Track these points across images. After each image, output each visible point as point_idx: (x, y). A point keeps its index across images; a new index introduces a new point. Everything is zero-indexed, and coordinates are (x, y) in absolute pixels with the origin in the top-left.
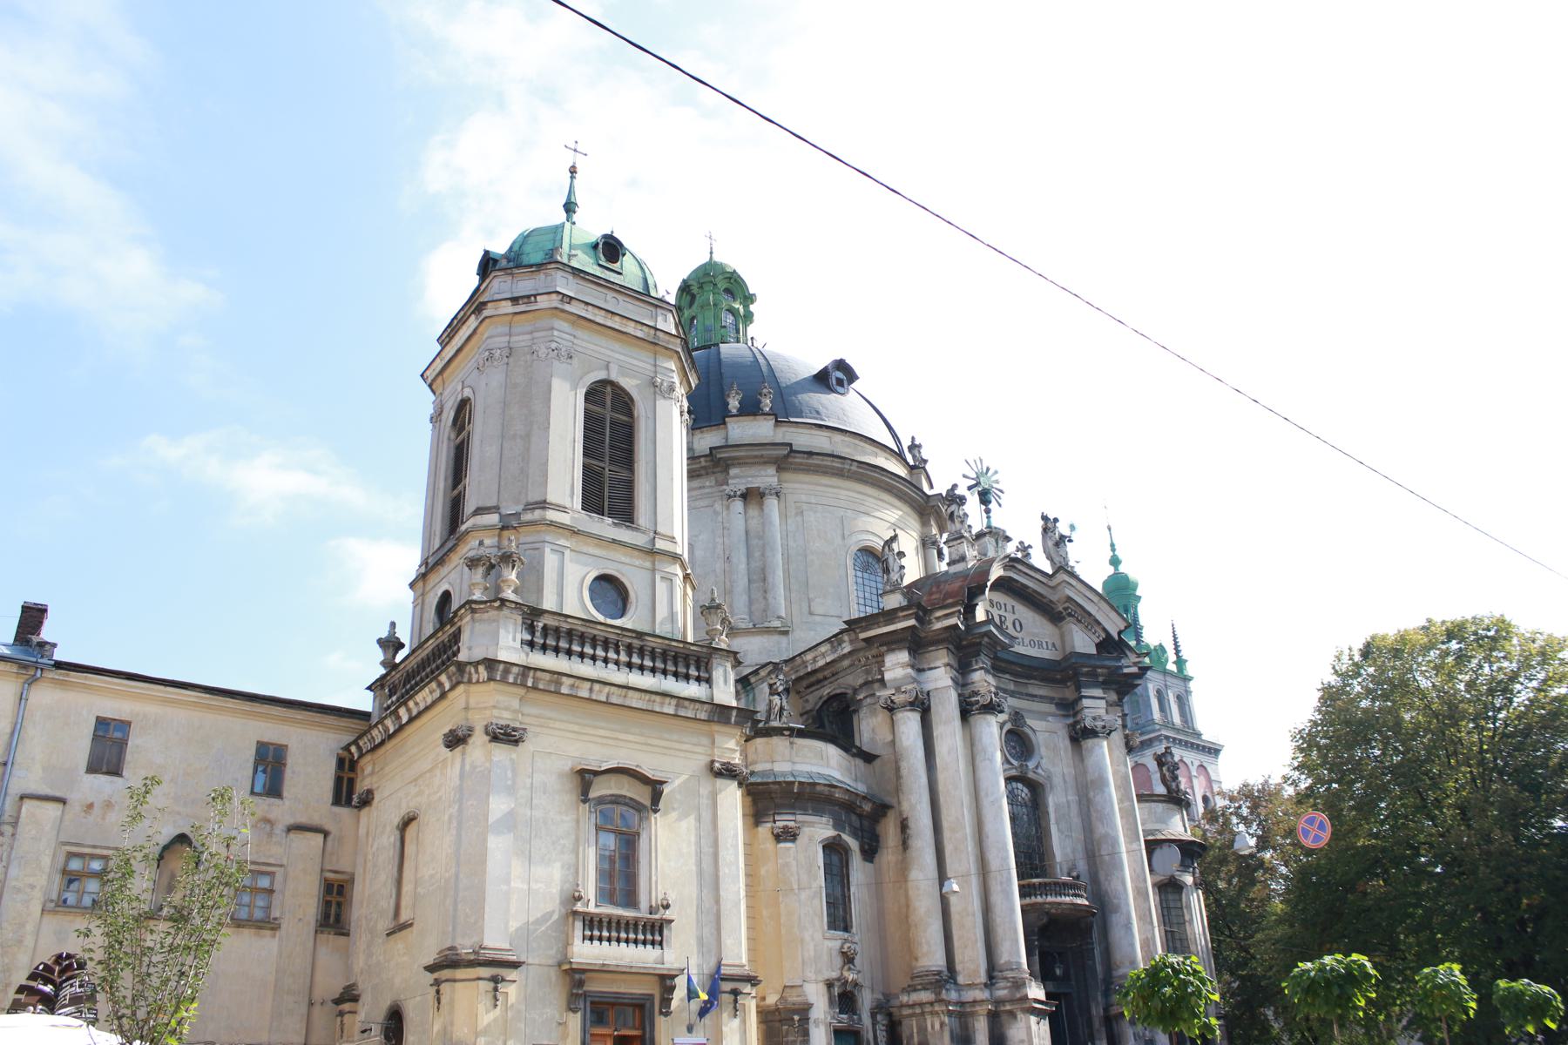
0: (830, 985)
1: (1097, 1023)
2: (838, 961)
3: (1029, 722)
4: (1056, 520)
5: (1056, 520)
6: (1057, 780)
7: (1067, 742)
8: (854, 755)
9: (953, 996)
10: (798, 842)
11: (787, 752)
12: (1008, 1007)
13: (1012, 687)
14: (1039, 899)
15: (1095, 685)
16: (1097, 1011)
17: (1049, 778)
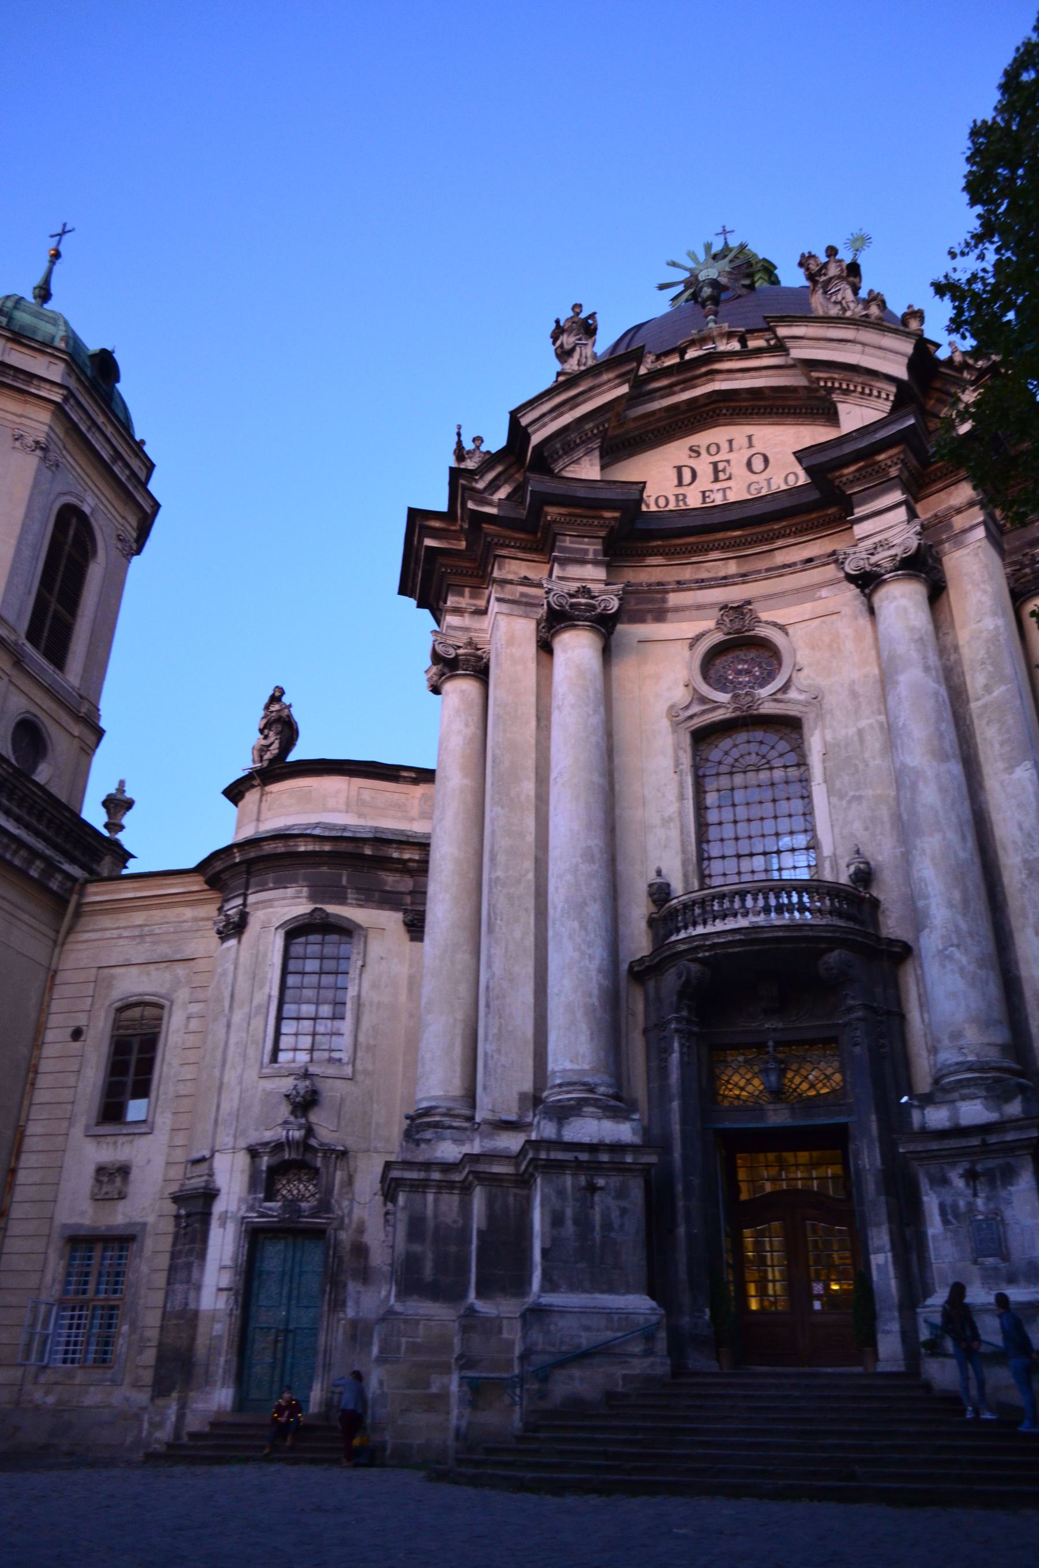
0: (253, 1152)
1: (871, 1186)
2: (284, 1111)
3: (764, 616)
4: (832, 251)
5: (832, 251)
6: (836, 700)
7: (864, 622)
8: (415, 782)
9: (448, 1150)
10: (245, 937)
11: (255, 808)
12: (523, 1167)
13: (732, 568)
14: (683, 935)
15: (885, 488)
16: (869, 1158)
17: (816, 699)
